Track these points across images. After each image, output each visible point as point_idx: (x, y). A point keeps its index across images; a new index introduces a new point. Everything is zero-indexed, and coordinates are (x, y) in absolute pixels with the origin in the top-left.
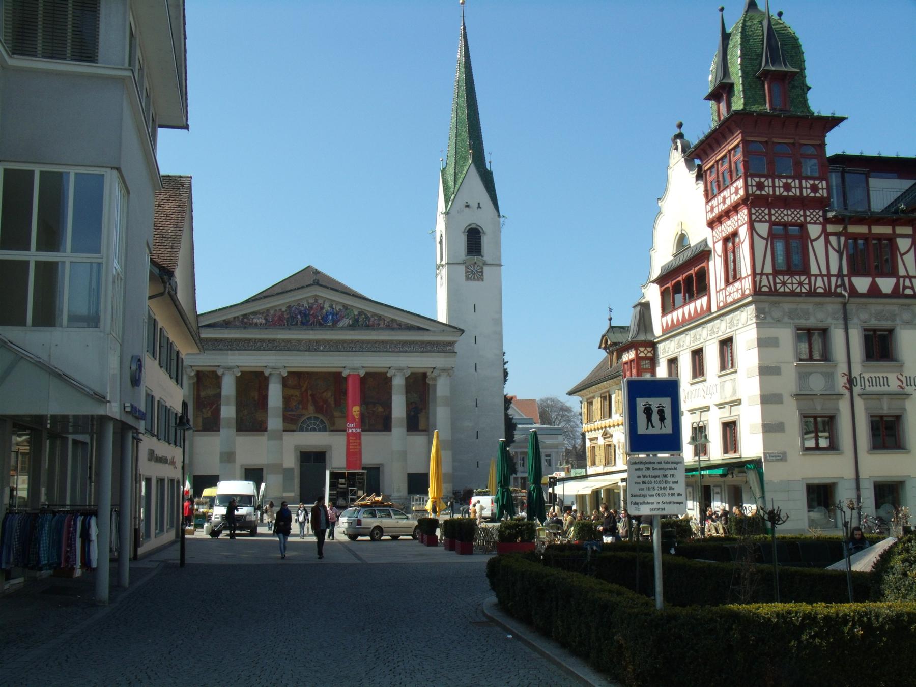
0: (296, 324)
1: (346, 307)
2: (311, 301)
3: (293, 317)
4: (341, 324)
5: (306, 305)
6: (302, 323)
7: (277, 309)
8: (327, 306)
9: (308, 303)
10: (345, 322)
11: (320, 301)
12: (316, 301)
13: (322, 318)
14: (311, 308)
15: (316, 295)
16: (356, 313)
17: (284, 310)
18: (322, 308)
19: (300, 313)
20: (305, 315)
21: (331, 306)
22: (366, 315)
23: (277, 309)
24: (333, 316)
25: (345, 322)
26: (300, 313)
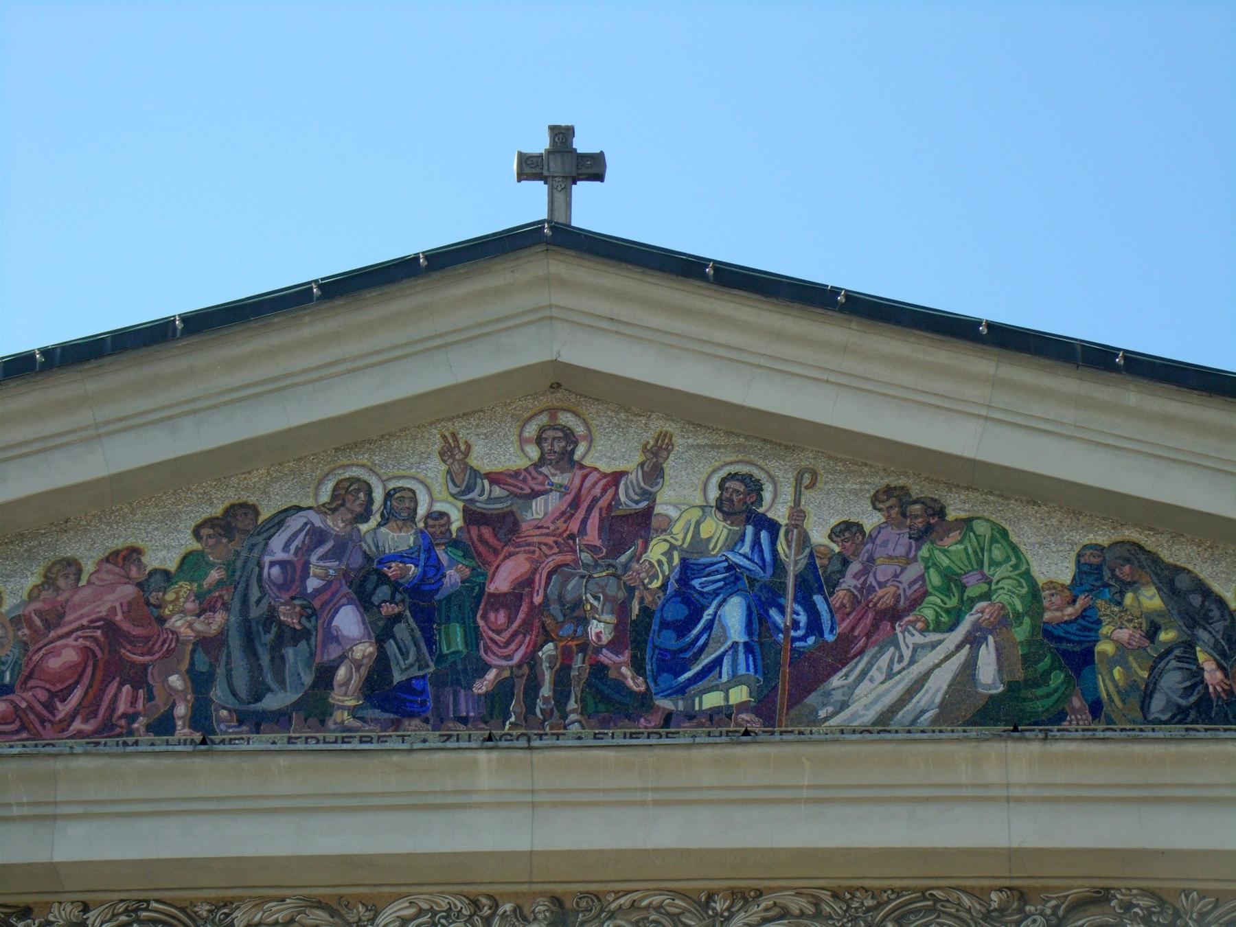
0: (314, 708)
1: (921, 498)
2: (501, 451)
3: (265, 637)
4: (866, 689)
5: (436, 497)
6: (391, 700)
7: (89, 552)
8: (686, 507)
9: (465, 479)
10: (927, 662)
11: (610, 451)
12: (561, 450)
13: (633, 633)
14: (493, 527)
15: (562, 381)
16: (1055, 567)
17: (164, 553)
18: (642, 523)
19: (365, 583)
20: (418, 601)
21: (740, 503)
22: (1170, 579)
23: (89, 552)
24: (763, 601)
25: (927, 662)
26: (365, 583)
